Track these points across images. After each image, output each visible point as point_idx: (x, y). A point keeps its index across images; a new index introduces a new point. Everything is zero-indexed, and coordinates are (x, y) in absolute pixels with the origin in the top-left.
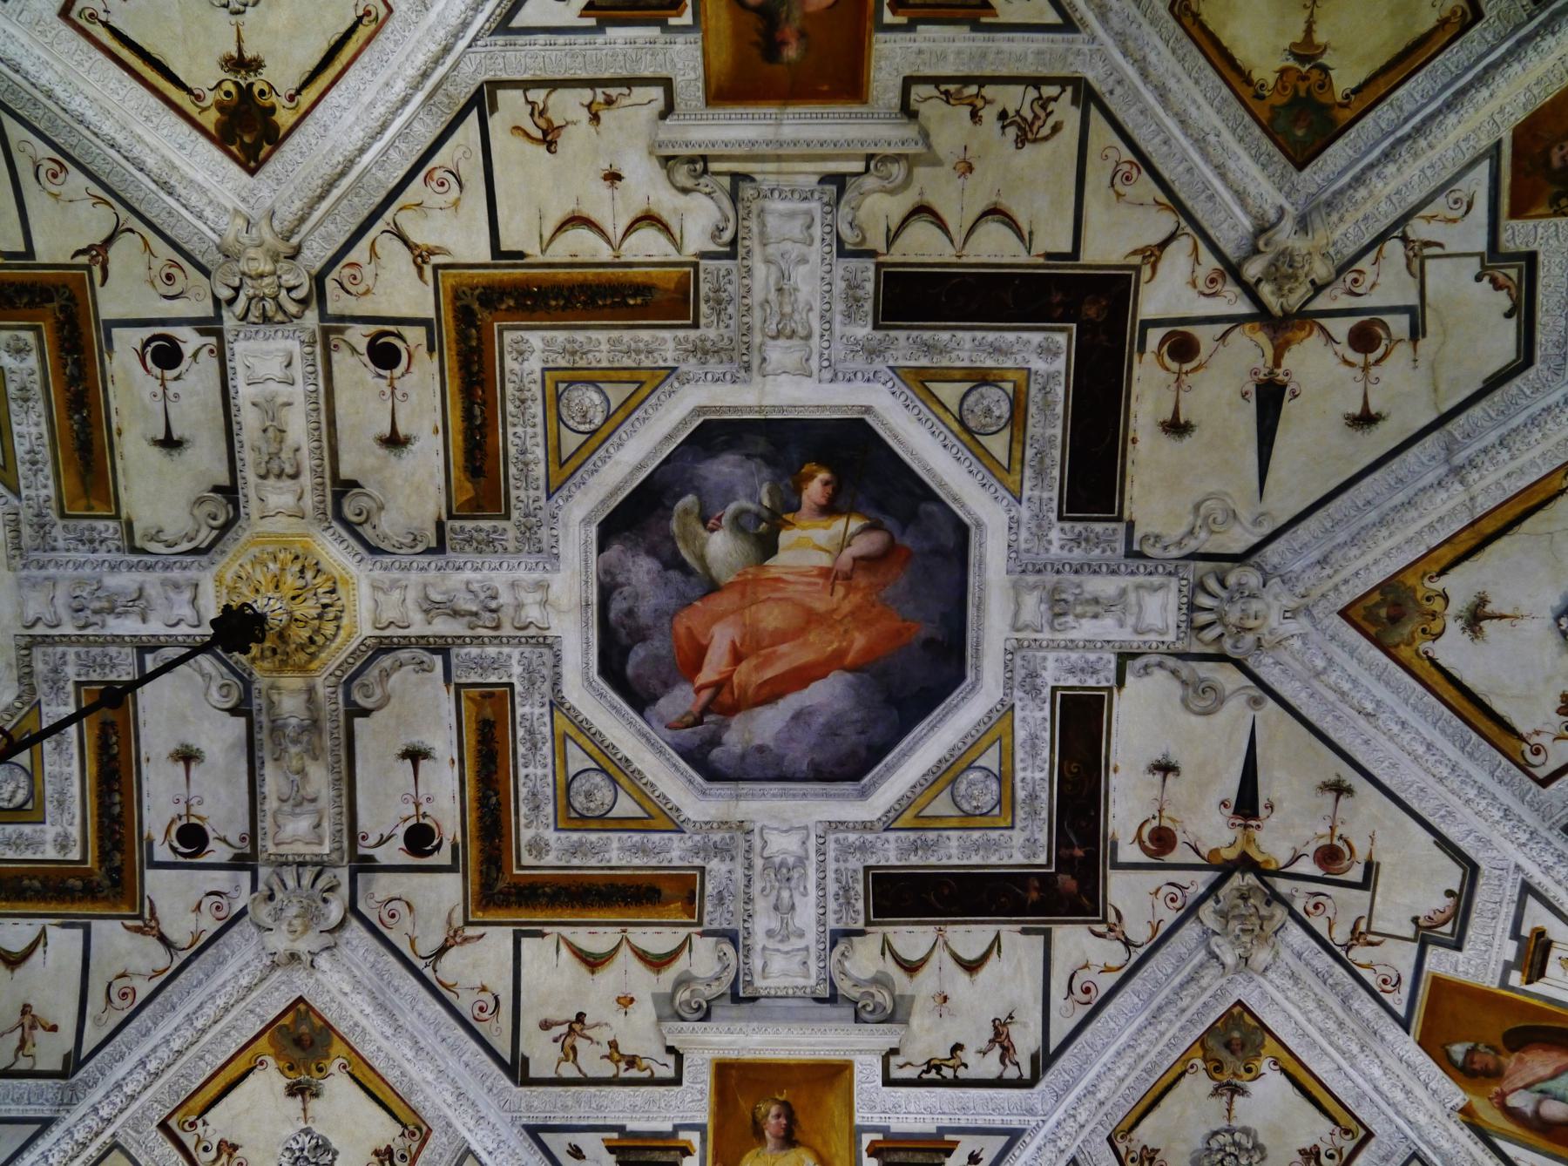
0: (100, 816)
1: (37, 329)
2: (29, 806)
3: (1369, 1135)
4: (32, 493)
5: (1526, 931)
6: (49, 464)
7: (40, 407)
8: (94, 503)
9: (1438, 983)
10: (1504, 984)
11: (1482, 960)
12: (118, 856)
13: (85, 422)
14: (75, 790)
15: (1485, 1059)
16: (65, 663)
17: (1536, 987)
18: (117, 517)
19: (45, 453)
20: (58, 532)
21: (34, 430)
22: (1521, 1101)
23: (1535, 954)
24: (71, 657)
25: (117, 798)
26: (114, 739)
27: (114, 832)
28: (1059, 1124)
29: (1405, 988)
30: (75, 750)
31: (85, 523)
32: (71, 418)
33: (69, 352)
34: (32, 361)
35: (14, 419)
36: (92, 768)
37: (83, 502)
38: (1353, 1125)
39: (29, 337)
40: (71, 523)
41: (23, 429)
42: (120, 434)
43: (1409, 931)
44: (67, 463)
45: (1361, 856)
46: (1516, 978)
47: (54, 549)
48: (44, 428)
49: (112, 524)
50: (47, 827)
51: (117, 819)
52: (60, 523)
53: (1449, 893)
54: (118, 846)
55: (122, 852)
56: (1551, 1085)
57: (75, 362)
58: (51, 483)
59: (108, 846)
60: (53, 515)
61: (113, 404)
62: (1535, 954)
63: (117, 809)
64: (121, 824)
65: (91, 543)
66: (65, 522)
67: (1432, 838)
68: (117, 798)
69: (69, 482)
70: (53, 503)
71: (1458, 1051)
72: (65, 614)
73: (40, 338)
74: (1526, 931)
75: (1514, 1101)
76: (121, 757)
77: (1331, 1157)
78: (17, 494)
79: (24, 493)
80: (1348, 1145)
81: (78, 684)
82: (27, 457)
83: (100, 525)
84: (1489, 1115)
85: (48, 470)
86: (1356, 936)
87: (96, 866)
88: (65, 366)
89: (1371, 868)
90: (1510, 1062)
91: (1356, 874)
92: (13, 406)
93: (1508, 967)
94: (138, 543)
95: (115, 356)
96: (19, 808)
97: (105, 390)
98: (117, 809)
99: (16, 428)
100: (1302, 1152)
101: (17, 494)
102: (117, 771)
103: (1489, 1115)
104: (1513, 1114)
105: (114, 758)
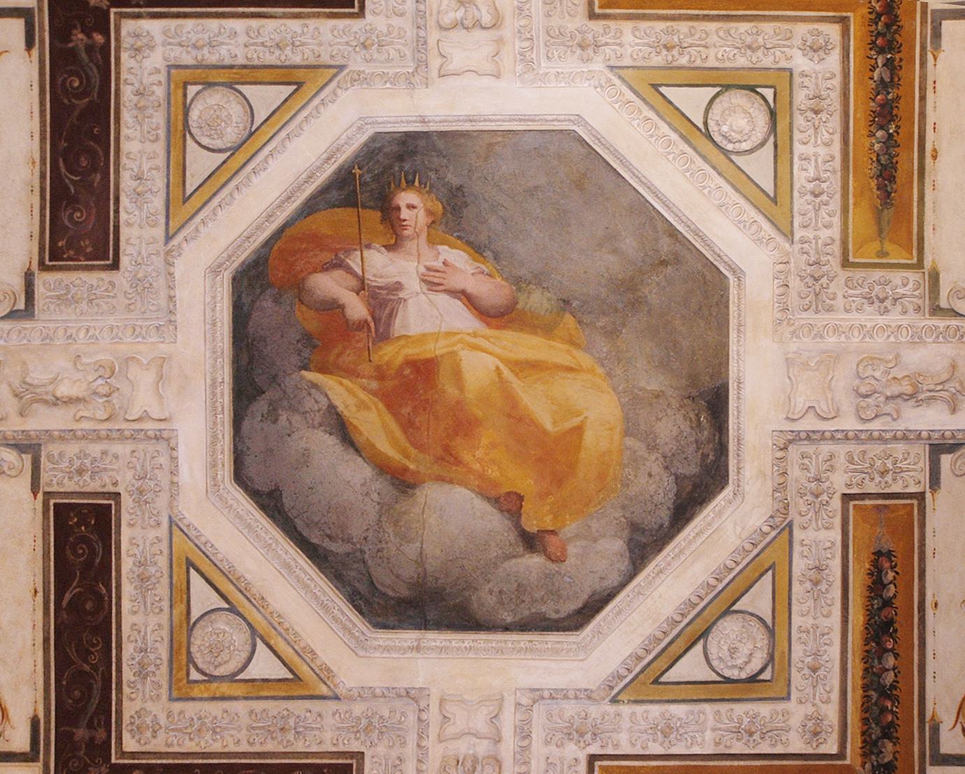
0: (865, 688)
1: (843, 21)
2: (766, 675)
4: (810, 234)
6: (838, 196)
7: (835, 123)
8: (888, 247)
12: (889, 746)
13: (890, 142)
14: (835, 651)
16: (832, 469)
18: (920, 265)
19: (833, 183)
20: (837, 287)
21: (822, 151)
24: (841, 460)
25: (890, 661)
26: (891, 575)
27: (883, 710)
30: (837, 593)
31: (877, 274)
32: (872, 135)
33: (881, 51)
34: (833, 61)
35: (797, 136)
36: (857, 617)
37: (876, 245)
39: (833, 32)
40: (859, 274)
41: (809, 150)
42: (935, 157)
44: (860, 194)
47: (830, 309)
48: (837, 148)
49: (913, 276)
50: (792, 705)
51: (887, 693)
52: (843, 275)
54: (888, 732)
55: (896, 742)
57: (889, 64)
58: (837, 220)
59: (876, 731)
60: (835, 263)
61: (931, 118)
63: (889, 678)
64: (894, 699)
65: (881, 302)
66: (849, 273)
68: (890, 661)
69: (861, 218)
70: (836, 249)
72: (847, 403)
73: (845, 33)
76: (897, 603)
78: (789, 235)
79: (798, 234)
81: (846, 498)
82: (810, 186)
83: (897, 277)
85: (836, 204)
87: (859, 761)
88: (873, 69)
92: (799, 121)
94: (943, 303)
95: (941, 56)
96: (753, 679)
97: (923, 98)
98: (889, 678)
99: (799, 149)
101: (789, 235)
102: (891, 622)
105: (887, 603)
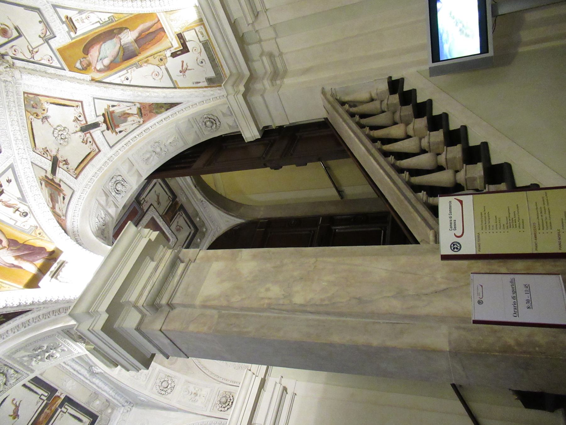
3: (82, 102)
5: (64, 20)
9: (59, 50)
10: (72, 39)
11: (62, 38)
15: (85, 62)
17: (79, 33)
22: (99, 66)
23: (71, 24)
28: (18, 154)
29: (54, 58)
38: (77, 104)
43: (41, 41)
45: (12, 27)
46: (73, 34)
53: (40, 22)
56: (100, 56)
62: (71, 24)
67: (22, 8)
71: (78, 65)
74: (64, 20)
75: (98, 68)
77: (80, 116)
80: (80, 109)
84: (98, 76)
86: (31, 52)
89: (16, 29)
90: (89, 58)
91: (15, 34)
93: (69, 33)
100: (74, 121)
103: (98, 76)
104: (100, 71)
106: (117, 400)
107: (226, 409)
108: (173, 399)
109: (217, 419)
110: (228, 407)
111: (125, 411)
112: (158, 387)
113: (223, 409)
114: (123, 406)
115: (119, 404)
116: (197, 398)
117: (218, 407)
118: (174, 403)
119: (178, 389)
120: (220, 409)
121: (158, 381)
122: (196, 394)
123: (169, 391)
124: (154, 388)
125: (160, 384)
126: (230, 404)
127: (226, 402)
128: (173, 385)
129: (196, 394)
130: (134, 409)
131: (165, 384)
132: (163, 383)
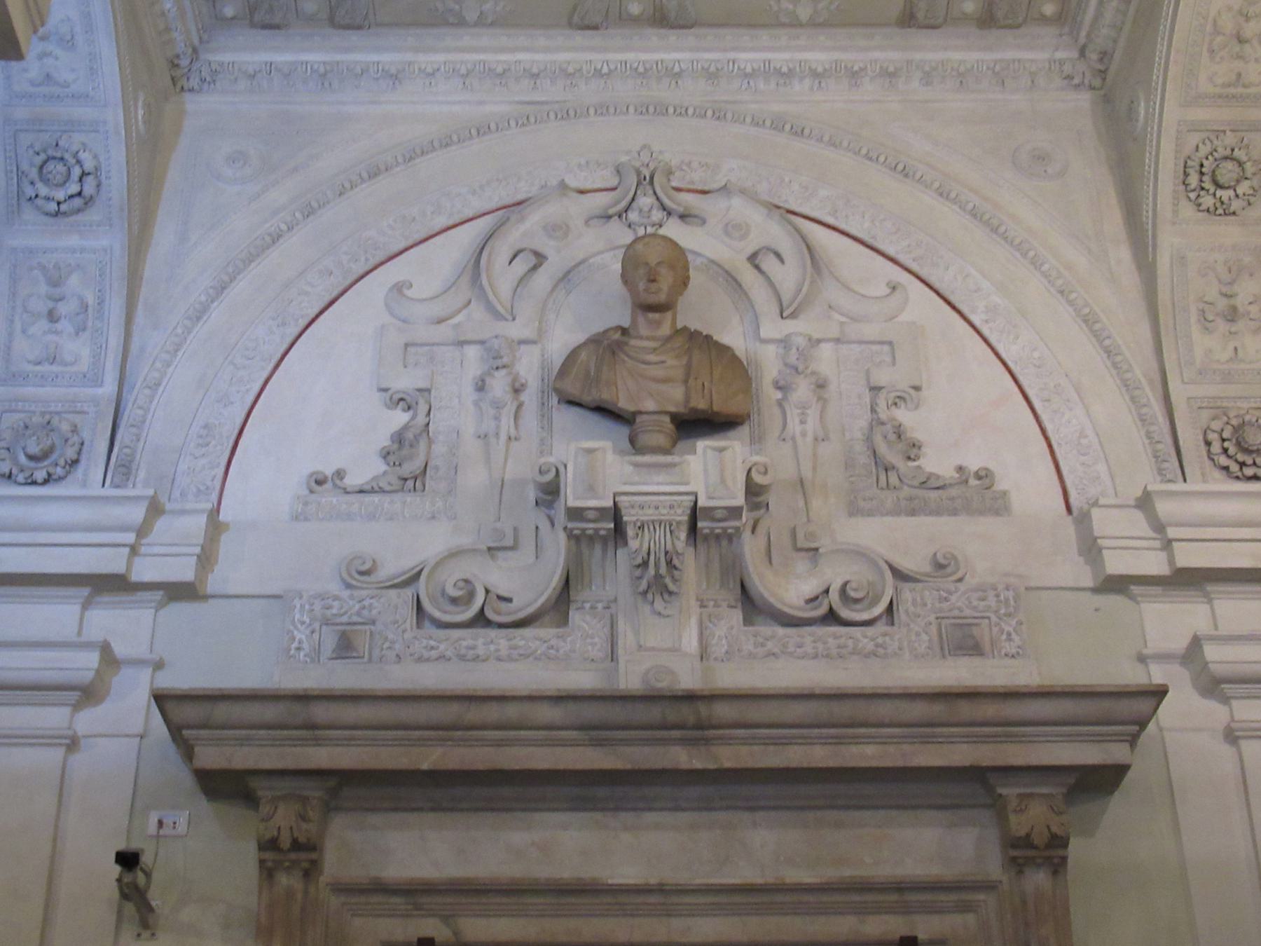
106: (1096, 19)
107: (1223, 460)
108: (1183, 234)
109: (1169, 440)
110: (1234, 468)
111: (1067, 68)
112: (1204, 150)
113: (1216, 448)
114: (1082, 53)
115: (1083, 33)
116: (1222, 326)
117: (1216, 425)
118: (1168, 242)
119: (1229, 233)
120: (1213, 436)
121: (1230, 139)
122: (1232, 315)
123: (1208, 201)
124: (1194, 139)
125: (1221, 152)
126: (1249, 471)
127: (1248, 451)
128: (1236, 205)
129: (1232, 315)
130: (1084, 99)
131: (1227, 172)
132: (1230, 165)
